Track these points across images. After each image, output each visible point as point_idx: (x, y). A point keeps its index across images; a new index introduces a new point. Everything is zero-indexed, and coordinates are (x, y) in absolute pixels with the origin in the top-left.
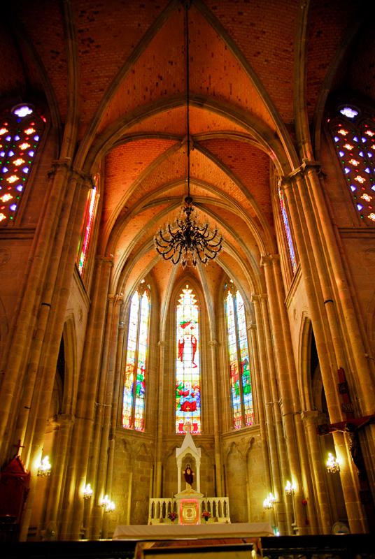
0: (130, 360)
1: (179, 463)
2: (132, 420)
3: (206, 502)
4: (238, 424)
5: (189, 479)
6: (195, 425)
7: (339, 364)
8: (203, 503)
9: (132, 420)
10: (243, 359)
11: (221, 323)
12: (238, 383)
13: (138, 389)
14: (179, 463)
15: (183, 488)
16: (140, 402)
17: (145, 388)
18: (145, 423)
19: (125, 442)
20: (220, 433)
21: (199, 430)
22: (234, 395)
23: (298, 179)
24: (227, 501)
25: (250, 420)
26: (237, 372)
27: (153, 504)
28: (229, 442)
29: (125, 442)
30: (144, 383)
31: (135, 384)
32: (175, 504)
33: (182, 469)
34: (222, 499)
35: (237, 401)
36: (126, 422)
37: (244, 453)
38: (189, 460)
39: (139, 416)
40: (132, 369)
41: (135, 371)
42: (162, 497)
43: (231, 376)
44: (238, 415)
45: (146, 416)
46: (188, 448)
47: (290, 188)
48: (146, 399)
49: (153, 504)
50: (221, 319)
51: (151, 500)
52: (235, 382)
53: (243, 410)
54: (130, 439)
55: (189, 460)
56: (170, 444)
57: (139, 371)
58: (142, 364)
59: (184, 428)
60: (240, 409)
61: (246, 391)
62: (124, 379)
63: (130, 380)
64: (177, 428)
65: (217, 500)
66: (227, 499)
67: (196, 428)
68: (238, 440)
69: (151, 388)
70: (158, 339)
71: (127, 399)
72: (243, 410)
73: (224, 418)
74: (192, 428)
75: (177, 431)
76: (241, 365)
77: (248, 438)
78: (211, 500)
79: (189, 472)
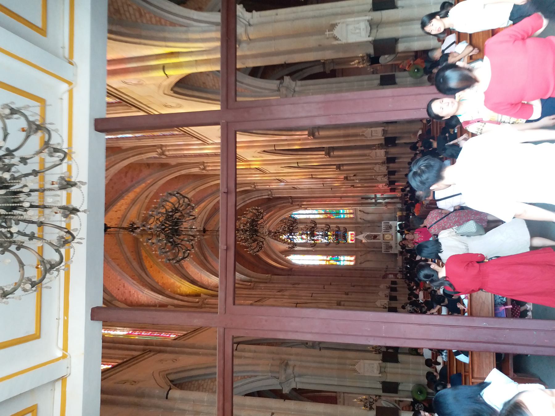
0: (324, 263)
1: (369, 241)
2: (351, 261)
3: (384, 230)
4: (352, 216)
5: (375, 237)
6: (351, 234)
7: (360, 198)
8: (384, 232)
9: (351, 261)
10: (323, 212)
11: (303, 221)
12: (334, 215)
13: (336, 259)
14: (369, 241)
15: (379, 239)
16: (342, 258)
17: (336, 256)
18: (351, 256)
19: (361, 263)
20: (355, 223)
21: (353, 232)
22: (339, 217)
23: (293, 200)
24: (384, 222)
25: (351, 211)
26: (329, 215)
27: (384, 251)
28: (359, 220)
29: (361, 263)
30: (333, 256)
31: (335, 260)
32: (384, 243)
33: (372, 240)
34: (383, 224)
35: (342, 216)
36: (352, 263)
37: (365, 214)
38: (368, 237)
39: (349, 258)
40: (328, 262)
41: (329, 261)
42: (382, 248)
43: (330, 218)
44: (348, 216)
45: (348, 255)
46: (361, 237)
47: (295, 202)
48: (341, 255)
49: (384, 251)
50: (301, 221)
51: (383, 252)
52: (333, 216)
53: (347, 214)
54: (359, 261)
55: (368, 237)
56: (360, 245)
57: (328, 259)
58: (325, 258)
59: (352, 239)
60: (346, 215)
61: (338, 212)
62: (333, 265)
63: (332, 262)
64: (352, 242)
65: (383, 226)
66: (383, 222)
67: (353, 234)
68: (359, 216)
69: (335, 253)
70: (312, 251)
71: (342, 263)
72: (347, 214)
73: (349, 222)
74: (352, 235)
75: (354, 242)
76: (326, 213)
77: (359, 213)
78: (383, 228)
79: (373, 237)
